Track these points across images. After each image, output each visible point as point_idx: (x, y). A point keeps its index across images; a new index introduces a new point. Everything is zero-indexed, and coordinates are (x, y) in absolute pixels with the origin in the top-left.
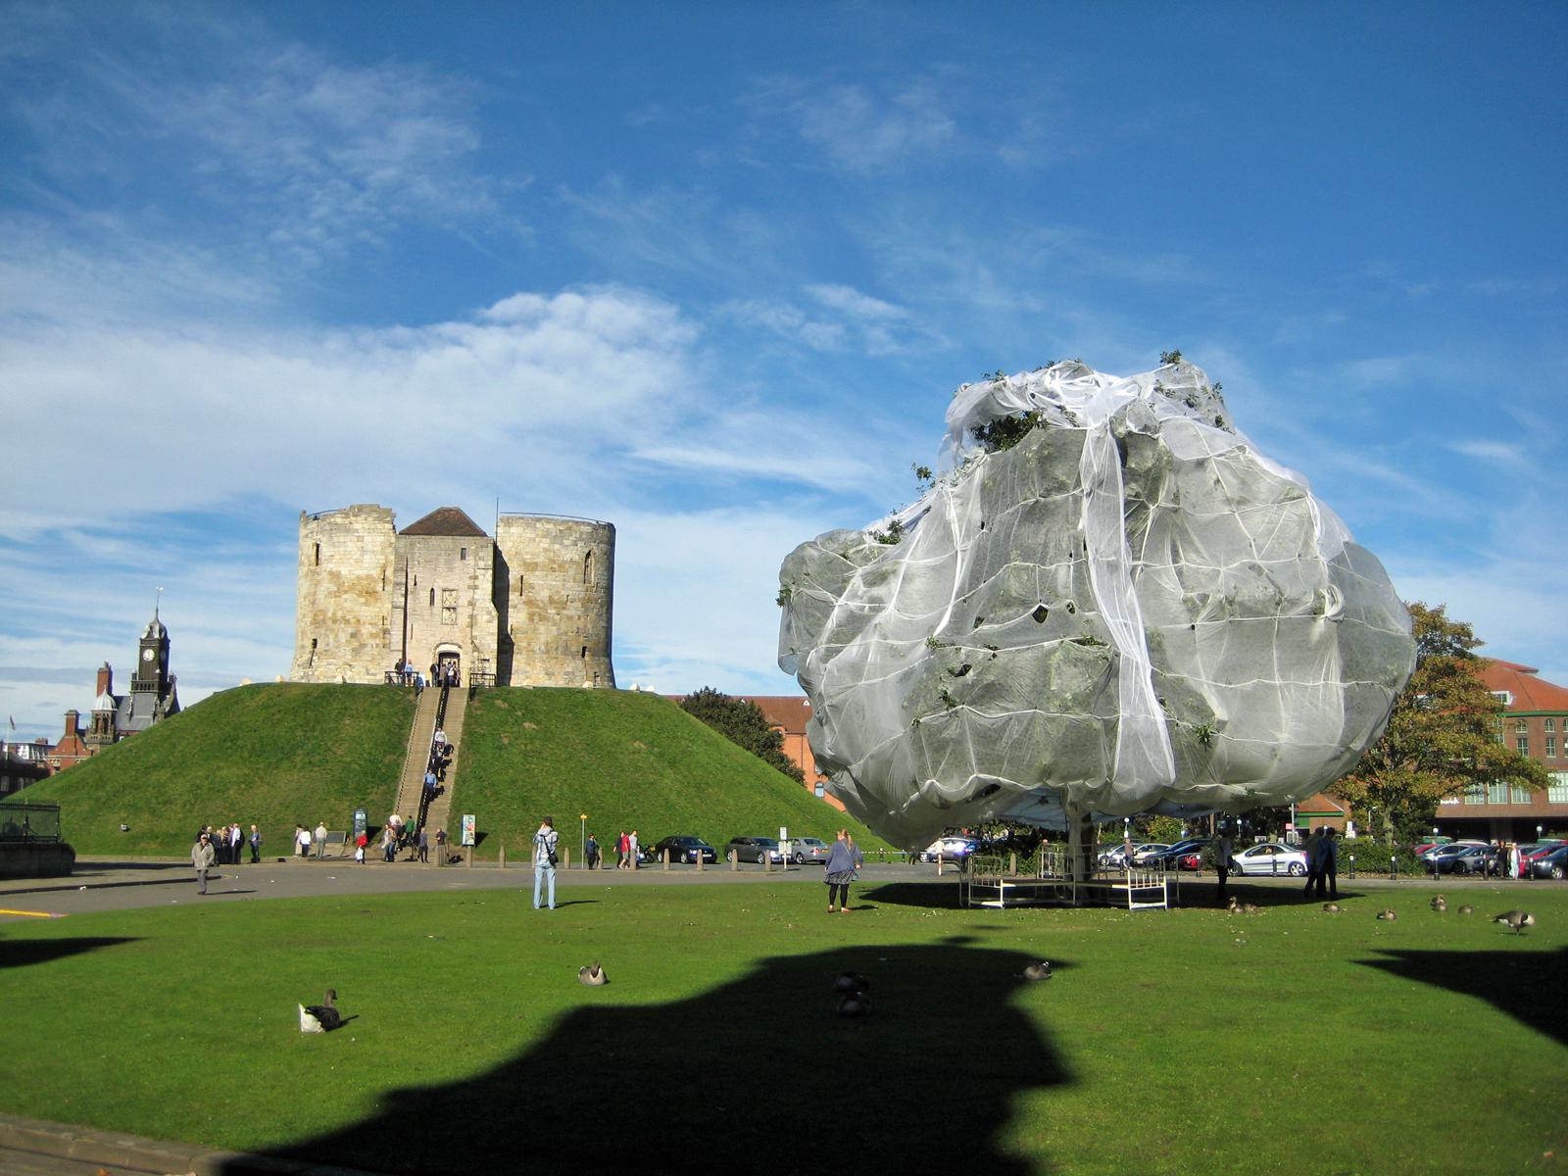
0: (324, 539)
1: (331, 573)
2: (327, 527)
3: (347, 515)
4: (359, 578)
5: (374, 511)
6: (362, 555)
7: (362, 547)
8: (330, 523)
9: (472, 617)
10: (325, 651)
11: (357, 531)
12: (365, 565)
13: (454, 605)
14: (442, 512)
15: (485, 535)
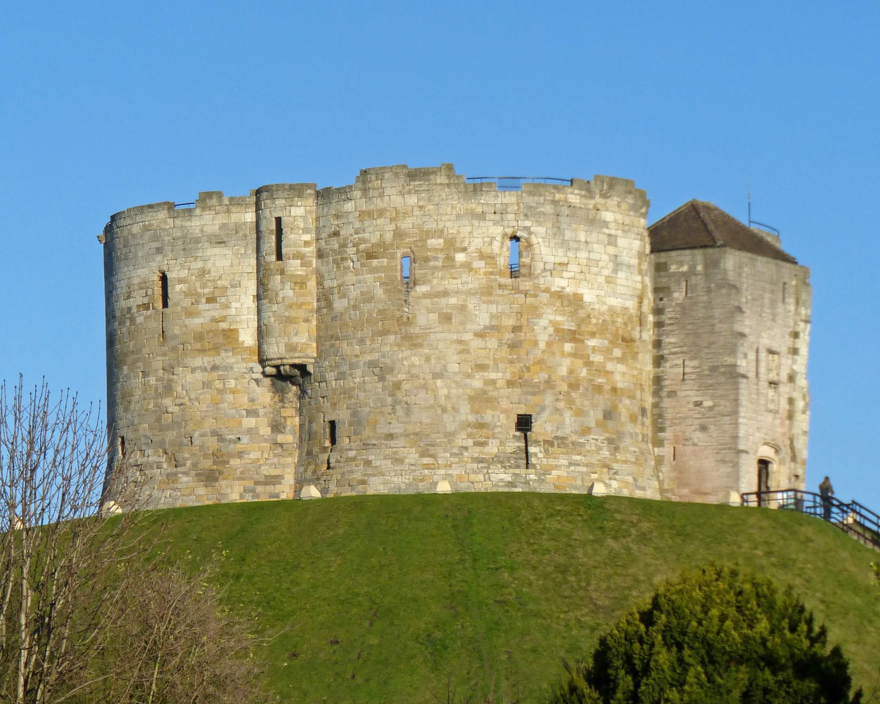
0: (541, 230)
1: (559, 295)
2: (549, 209)
3: (587, 188)
4: (612, 310)
5: (630, 193)
6: (615, 271)
7: (616, 256)
8: (555, 203)
9: (791, 401)
10: (556, 438)
11: (606, 224)
12: (620, 290)
13: (776, 379)
14: (694, 210)
15: (796, 263)
